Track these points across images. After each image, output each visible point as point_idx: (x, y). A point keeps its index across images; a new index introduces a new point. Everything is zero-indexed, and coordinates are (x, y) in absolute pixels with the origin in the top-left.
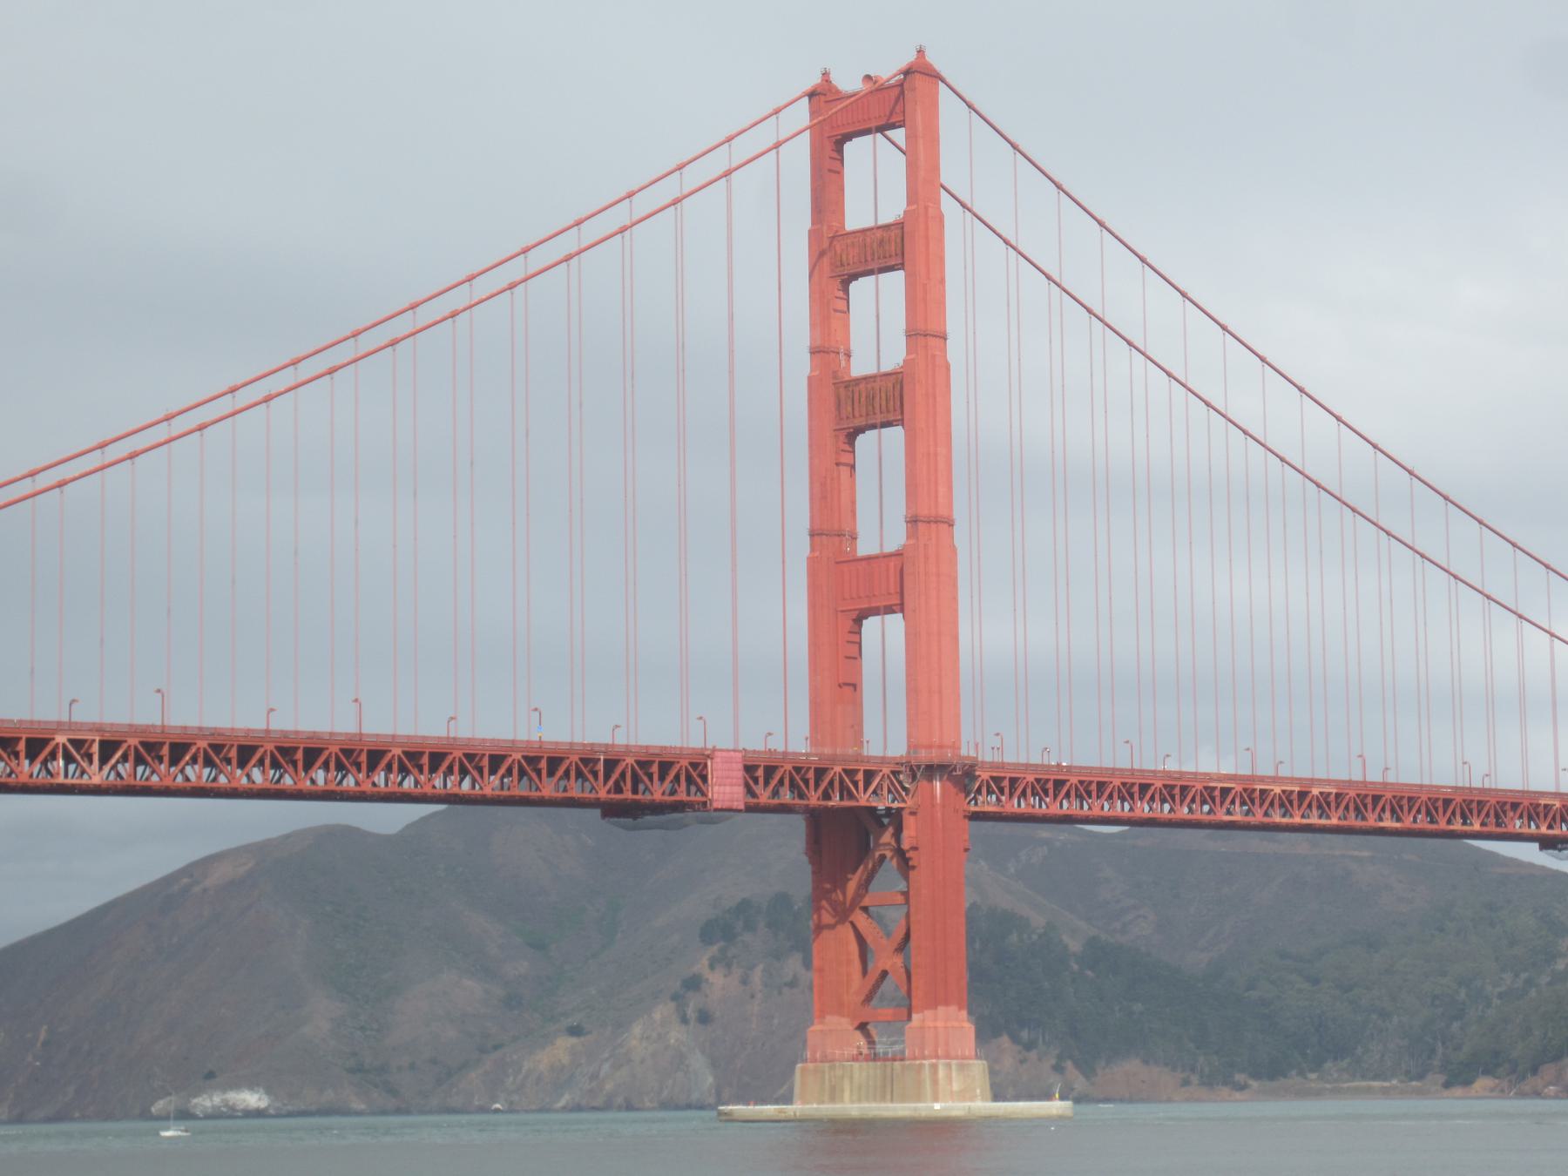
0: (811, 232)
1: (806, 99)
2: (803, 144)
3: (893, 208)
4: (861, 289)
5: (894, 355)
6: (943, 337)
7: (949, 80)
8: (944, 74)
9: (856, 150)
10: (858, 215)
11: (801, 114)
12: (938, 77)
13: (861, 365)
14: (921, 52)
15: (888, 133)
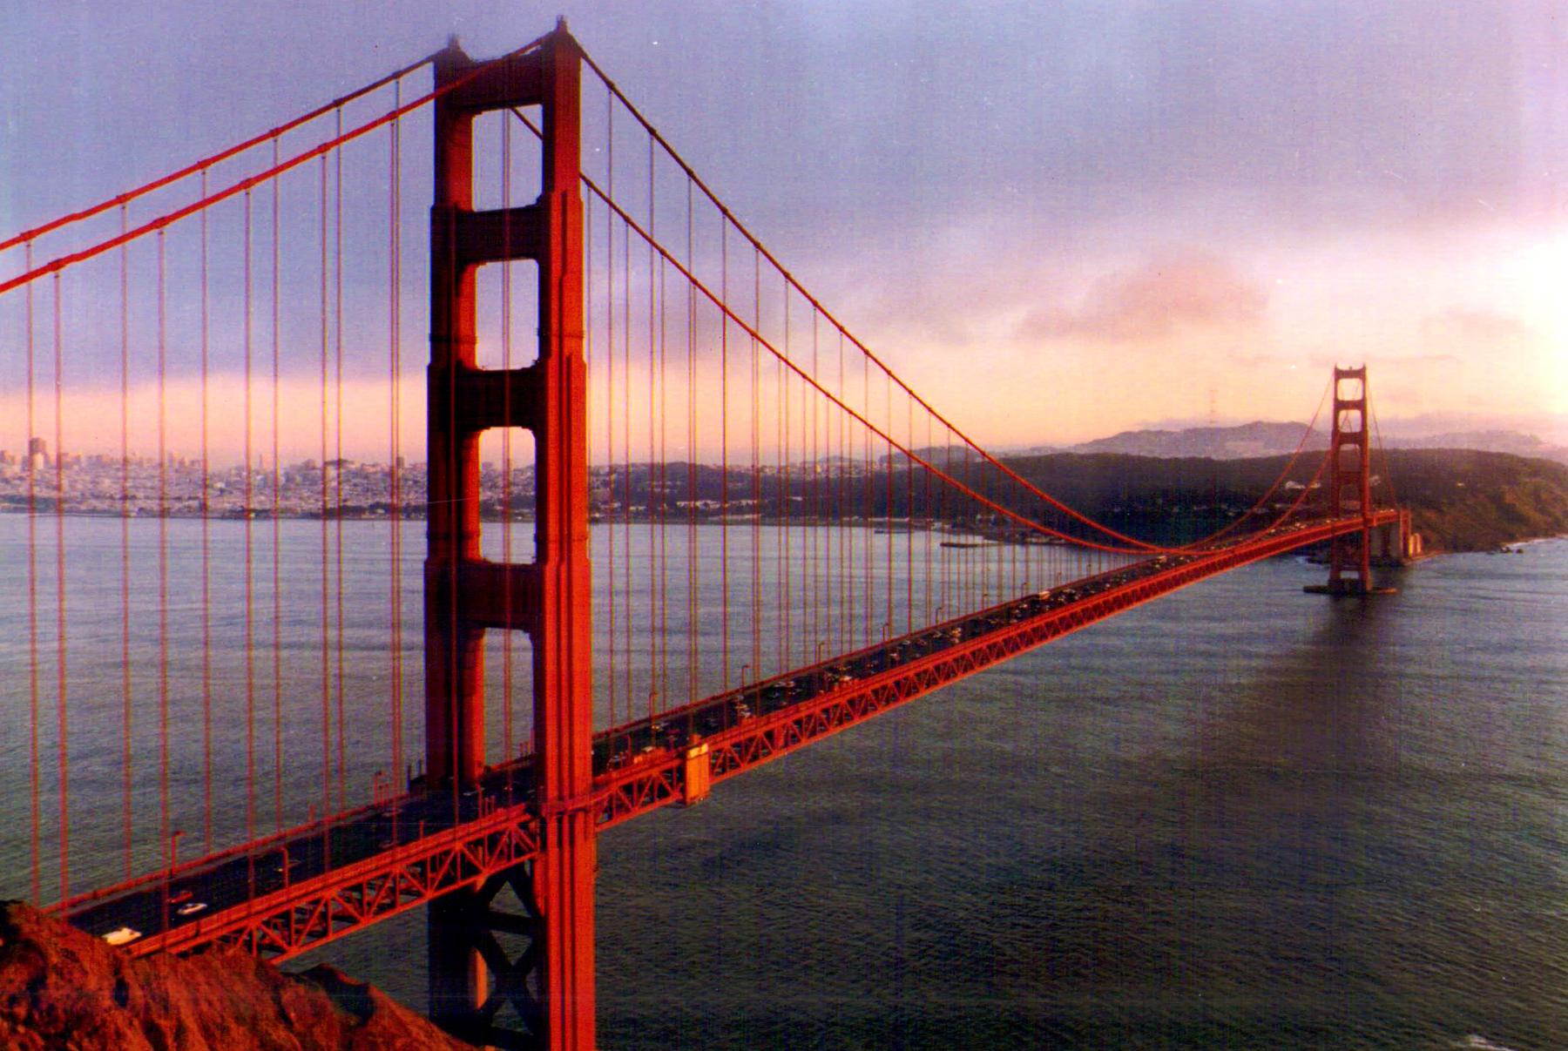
0: (435, 211)
1: (430, 65)
2: (425, 116)
3: (526, 190)
4: (487, 277)
5: (525, 354)
6: (579, 336)
7: (590, 56)
8: (585, 49)
9: (486, 126)
10: (485, 196)
11: (423, 82)
12: (576, 53)
13: (488, 354)
14: (561, 24)
15: (518, 109)
